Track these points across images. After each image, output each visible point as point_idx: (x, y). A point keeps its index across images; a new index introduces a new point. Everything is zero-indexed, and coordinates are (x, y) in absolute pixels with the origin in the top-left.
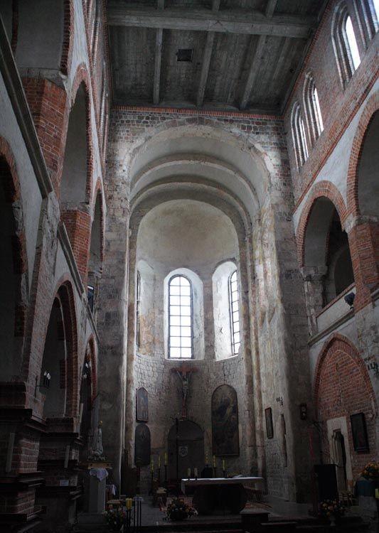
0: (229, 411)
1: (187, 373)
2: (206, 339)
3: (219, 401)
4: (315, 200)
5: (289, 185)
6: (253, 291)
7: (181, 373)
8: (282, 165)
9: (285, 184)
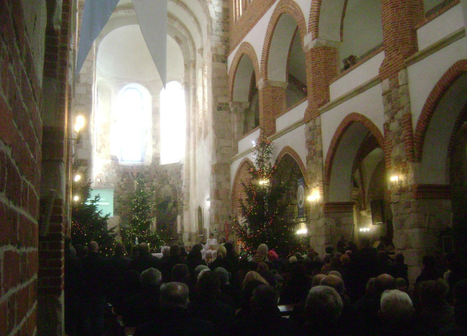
0: (170, 205)
1: (138, 174)
2: (155, 146)
3: (163, 197)
4: (243, 54)
5: (227, 31)
6: (194, 111)
7: (132, 173)
8: (222, 13)
9: (223, 31)
